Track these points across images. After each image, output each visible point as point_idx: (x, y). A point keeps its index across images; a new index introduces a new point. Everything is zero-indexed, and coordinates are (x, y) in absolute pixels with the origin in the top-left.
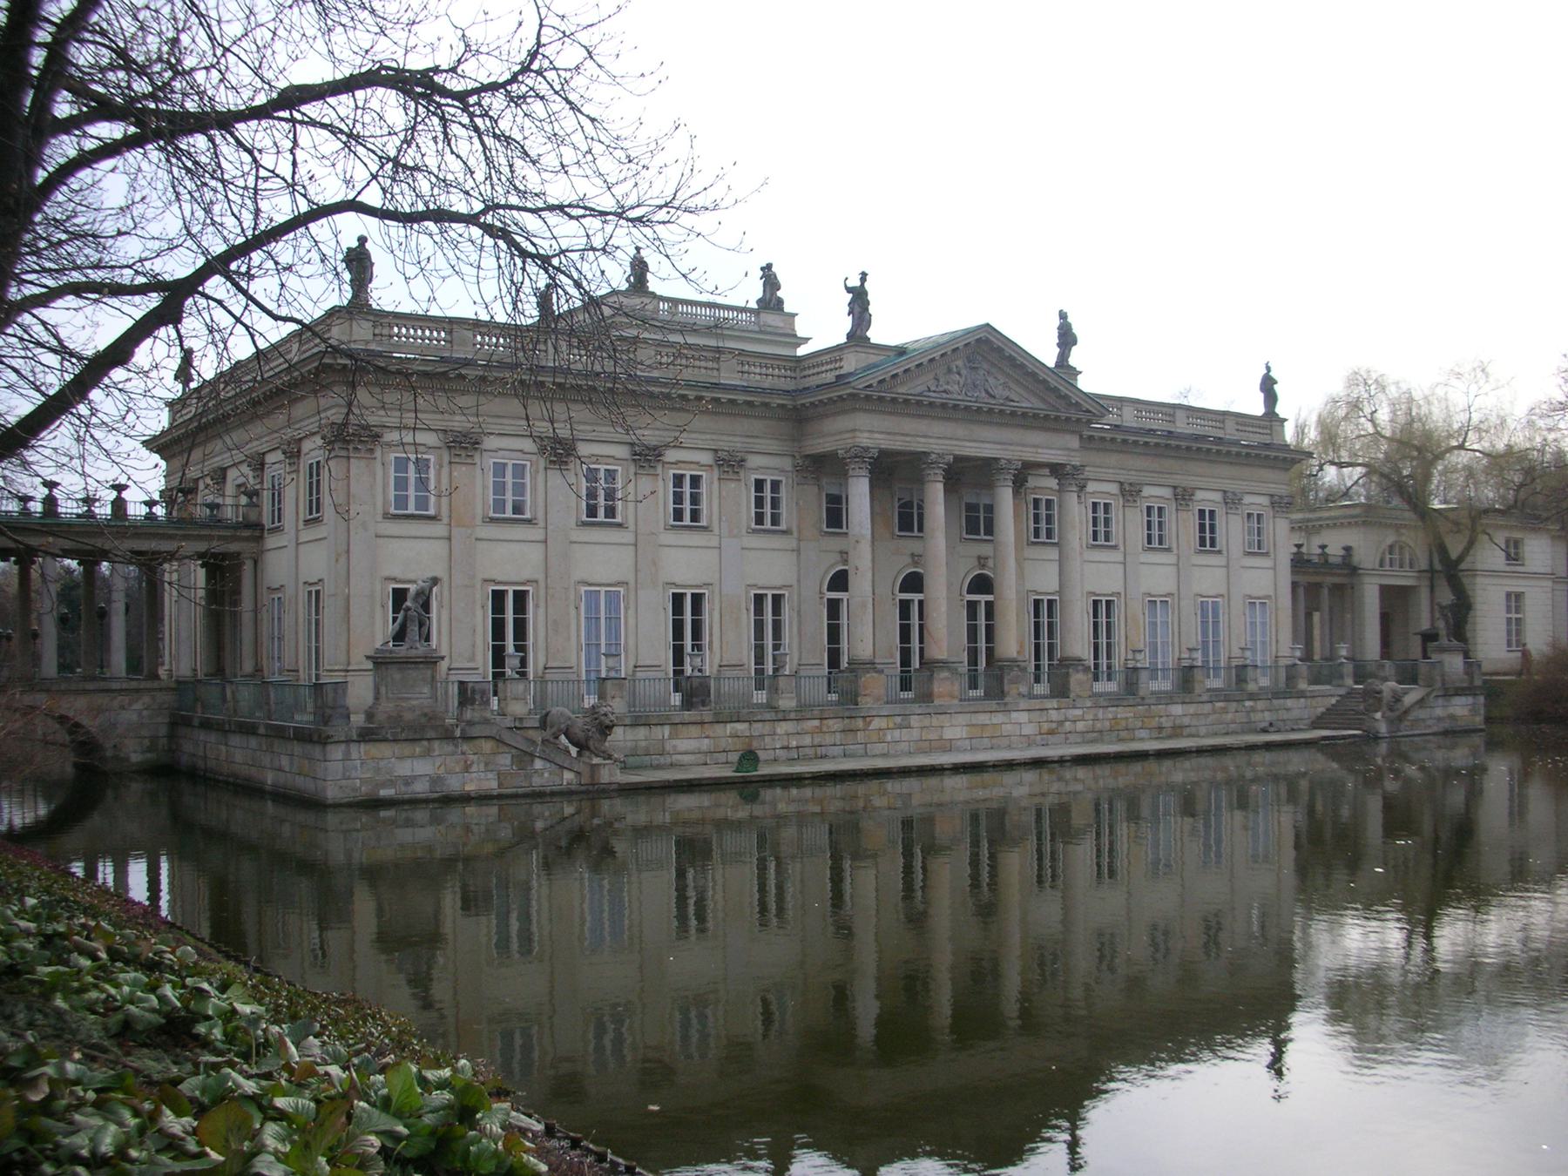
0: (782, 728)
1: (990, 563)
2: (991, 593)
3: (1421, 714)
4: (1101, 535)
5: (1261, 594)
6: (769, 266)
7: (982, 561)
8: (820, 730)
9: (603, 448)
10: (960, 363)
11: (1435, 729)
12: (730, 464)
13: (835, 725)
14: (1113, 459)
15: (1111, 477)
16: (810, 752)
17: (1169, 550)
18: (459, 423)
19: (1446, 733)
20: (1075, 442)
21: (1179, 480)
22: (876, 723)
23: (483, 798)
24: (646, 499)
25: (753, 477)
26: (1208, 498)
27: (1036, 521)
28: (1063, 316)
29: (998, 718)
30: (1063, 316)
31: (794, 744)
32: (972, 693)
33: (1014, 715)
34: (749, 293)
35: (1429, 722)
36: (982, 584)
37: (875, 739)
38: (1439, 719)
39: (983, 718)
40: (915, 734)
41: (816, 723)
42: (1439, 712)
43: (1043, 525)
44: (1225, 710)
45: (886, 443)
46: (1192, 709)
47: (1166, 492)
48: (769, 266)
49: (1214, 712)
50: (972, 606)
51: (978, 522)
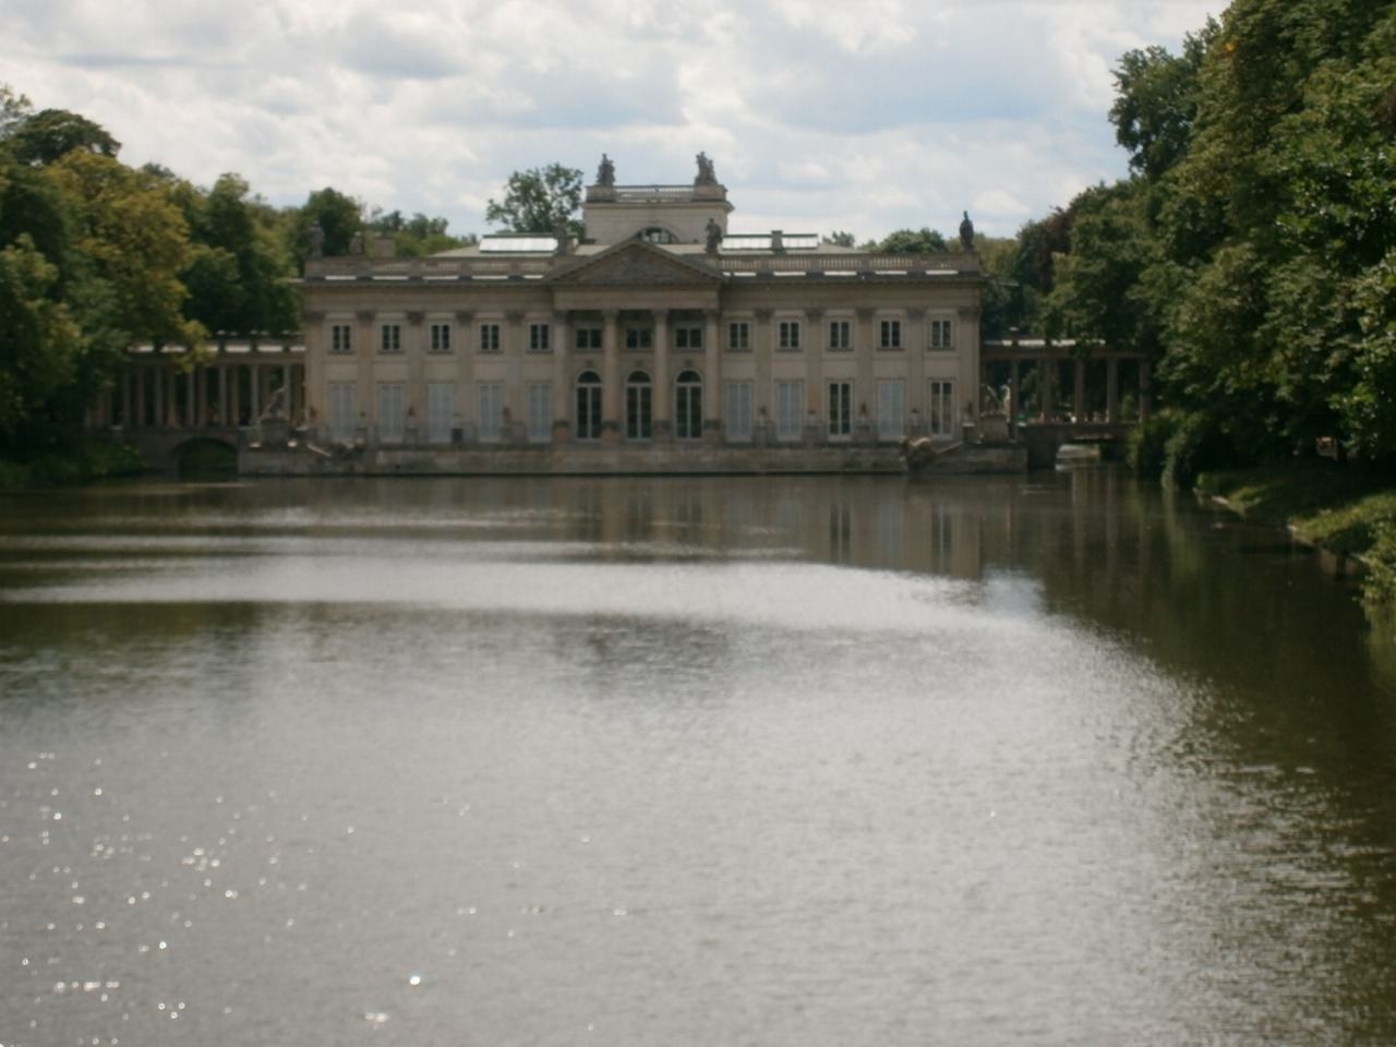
0: (500, 454)
6: (703, 153)
9: (440, 315)
10: (625, 258)
12: (515, 318)
17: (851, 350)
18: (364, 307)
20: (713, 295)
23: (302, 476)
24: (465, 338)
25: (530, 323)
26: (890, 312)
32: (682, 440)
34: (688, 175)
45: (572, 306)
48: (703, 153)
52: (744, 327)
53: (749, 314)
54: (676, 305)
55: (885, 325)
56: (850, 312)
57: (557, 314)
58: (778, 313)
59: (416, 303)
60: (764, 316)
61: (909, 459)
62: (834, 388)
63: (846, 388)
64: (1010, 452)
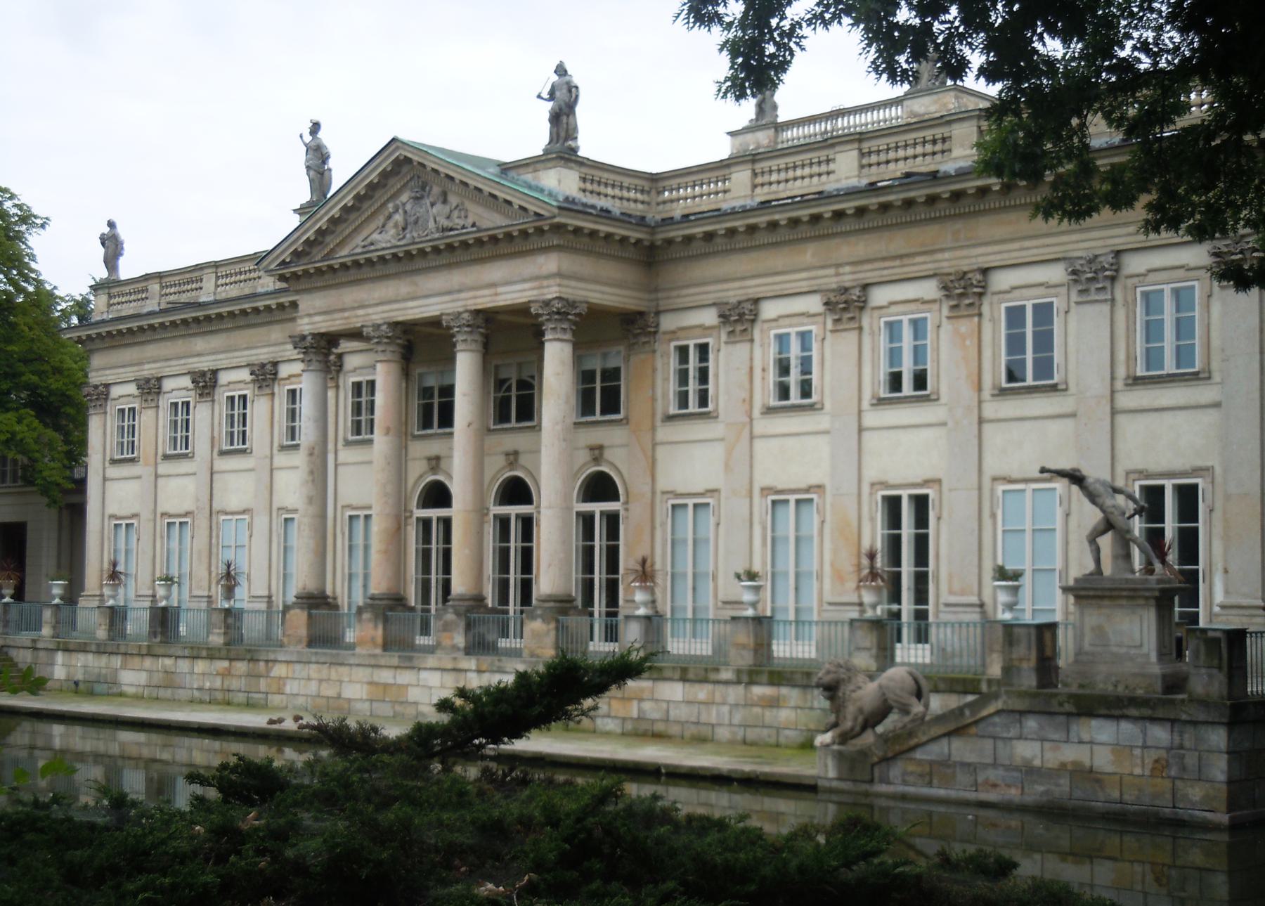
0: (200, 666)
1: (523, 460)
2: (615, 497)
3: (960, 749)
4: (794, 390)
5: (1179, 464)
7: (513, 457)
8: (226, 674)
10: (404, 197)
11: (1013, 794)
13: (241, 667)
14: (809, 254)
15: (804, 286)
16: (219, 696)
18: (148, 370)
19: (1051, 812)
21: (952, 261)
22: (279, 670)
27: (683, 377)
28: (561, 70)
29: (405, 677)
30: (561, 70)
31: (207, 685)
33: (424, 674)
35: (993, 775)
36: (516, 491)
37: (274, 688)
38: (1030, 772)
39: (386, 676)
40: (313, 687)
41: (226, 664)
42: (1027, 751)
43: (693, 386)
44: (774, 703)
46: (702, 692)
47: (929, 289)
49: (748, 704)
50: (587, 521)
51: (514, 403)
52: (703, 350)
53: (709, 317)
54: (485, 300)
55: (1015, 316)
56: (929, 289)
57: (299, 341)
58: (769, 310)
59: (205, 352)
60: (739, 319)
61: (844, 738)
62: (893, 505)
63: (921, 504)
64: (1160, 734)
